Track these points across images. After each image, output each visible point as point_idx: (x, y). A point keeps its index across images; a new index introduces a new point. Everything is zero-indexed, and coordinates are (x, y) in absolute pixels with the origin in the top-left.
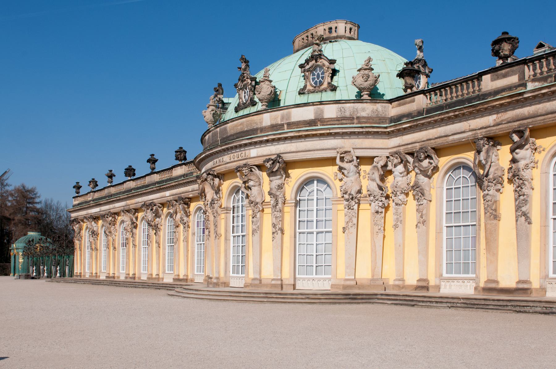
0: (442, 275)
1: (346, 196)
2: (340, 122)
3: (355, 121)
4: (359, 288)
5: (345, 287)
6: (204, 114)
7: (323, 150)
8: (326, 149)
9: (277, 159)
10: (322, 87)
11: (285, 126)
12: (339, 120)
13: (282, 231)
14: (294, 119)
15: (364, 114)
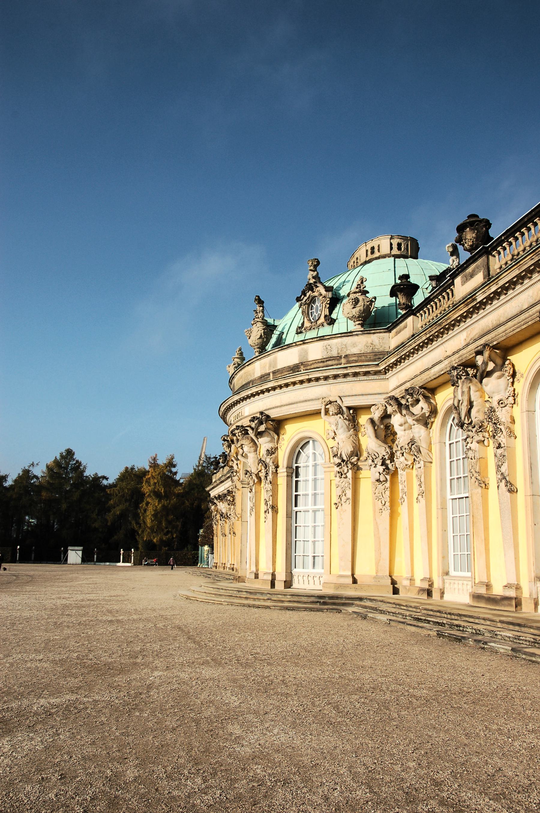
0: (447, 574)
1: (338, 461)
2: (325, 364)
3: (343, 361)
4: (356, 589)
5: (339, 586)
6: (228, 369)
7: (306, 401)
8: (309, 400)
9: (263, 418)
10: (319, 322)
11: (271, 374)
12: (323, 362)
13: (274, 508)
14: (280, 365)
15: (355, 351)
